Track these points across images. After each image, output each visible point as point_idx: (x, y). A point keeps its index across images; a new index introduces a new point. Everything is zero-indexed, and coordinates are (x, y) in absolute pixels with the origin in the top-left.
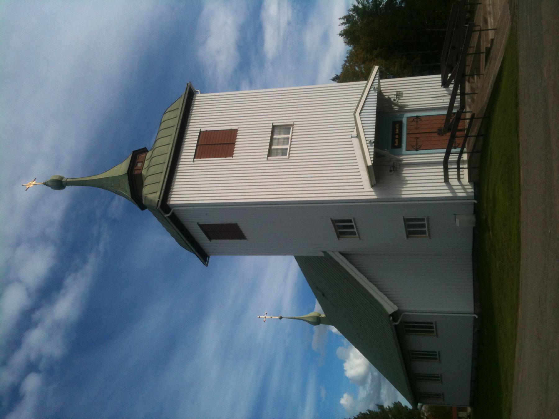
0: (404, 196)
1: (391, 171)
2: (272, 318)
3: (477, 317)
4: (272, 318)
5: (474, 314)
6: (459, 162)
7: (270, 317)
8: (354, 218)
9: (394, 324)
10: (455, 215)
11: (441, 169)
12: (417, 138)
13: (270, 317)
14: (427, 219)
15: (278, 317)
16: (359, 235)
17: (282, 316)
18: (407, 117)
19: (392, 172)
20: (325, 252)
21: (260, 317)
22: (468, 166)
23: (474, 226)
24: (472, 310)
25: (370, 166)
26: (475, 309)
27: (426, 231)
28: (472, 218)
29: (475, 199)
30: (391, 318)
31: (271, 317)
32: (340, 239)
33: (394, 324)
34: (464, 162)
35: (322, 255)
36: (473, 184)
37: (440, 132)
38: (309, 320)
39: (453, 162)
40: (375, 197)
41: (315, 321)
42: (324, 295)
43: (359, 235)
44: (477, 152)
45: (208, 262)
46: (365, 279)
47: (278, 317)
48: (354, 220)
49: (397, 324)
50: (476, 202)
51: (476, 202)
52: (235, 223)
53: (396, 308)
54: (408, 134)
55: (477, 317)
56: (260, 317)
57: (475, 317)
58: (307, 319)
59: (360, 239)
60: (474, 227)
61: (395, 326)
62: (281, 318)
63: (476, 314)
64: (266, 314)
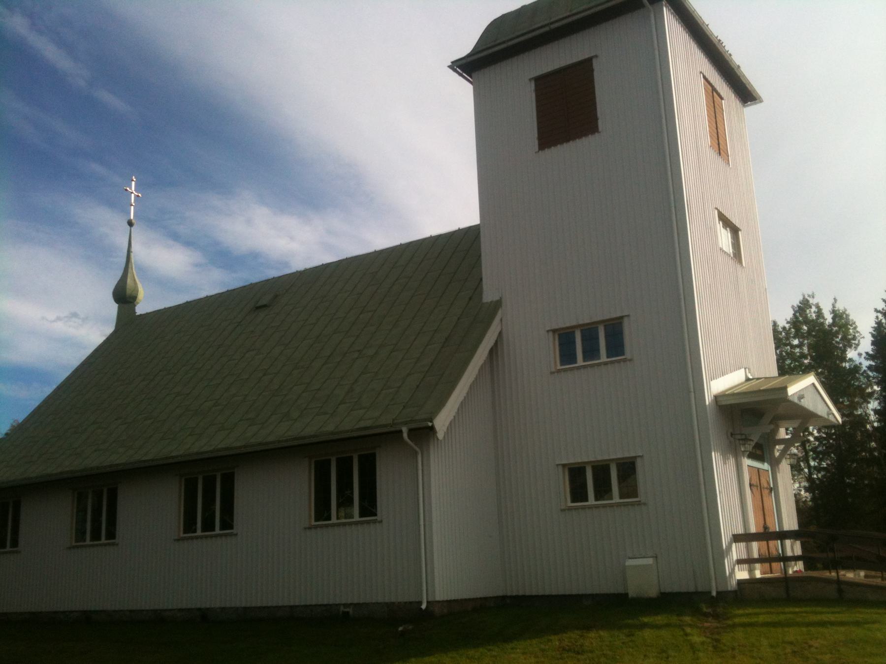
0: (713, 454)
1: (732, 434)
2: (132, 205)
3: (424, 606)
4: (132, 205)
5: (428, 602)
6: (785, 559)
7: (133, 201)
8: (630, 360)
9: (405, 430)
10: (656, 557)
11: (740, 531)
12: (757, 486)
13: (133, 201)
14: (640, 501)
15: (132, 218)
16: (559, 371)
17: (134, 227)
18: (768, 471)
19: (732, 439)
20: (497, 305)
21: (133, 180)
22: (761, 581)
23: (632, 594)
24: (440, 596)
25: (786, 393)
26: (439, 602)
27: (586, 500)
28: (653, 593)
29: (718, 593)
30: (430, 424)
31: (134, 204)
32: (551, 334)
33: (405, 430)
34: (751, 571)
35: (489, 295)
36: (736, 589)
37: (765, 527)
38: (129, 281)
39: (749, 550)
40: (707, 403)
41: (128, 292)
42: (265, 306)
43: (559, 371)
44: (840, 591)
45: (455, 71)
46: (471, 379)
47: (132, 218)
48: (625, 360)
49: (405, 435)
50: (714, 594)
51: (714, 594)
52: (600, 129)
53: (440, 435)
54: (758, 469)
55: (424, 606)
56: (133, 180)
57: (420, 603)
58: (129, 275)
59: (552, 373)
60: (627, 594)
61: (401, 432)
62: (130, 224)
63: (427, 607)
64: (138, 196)
